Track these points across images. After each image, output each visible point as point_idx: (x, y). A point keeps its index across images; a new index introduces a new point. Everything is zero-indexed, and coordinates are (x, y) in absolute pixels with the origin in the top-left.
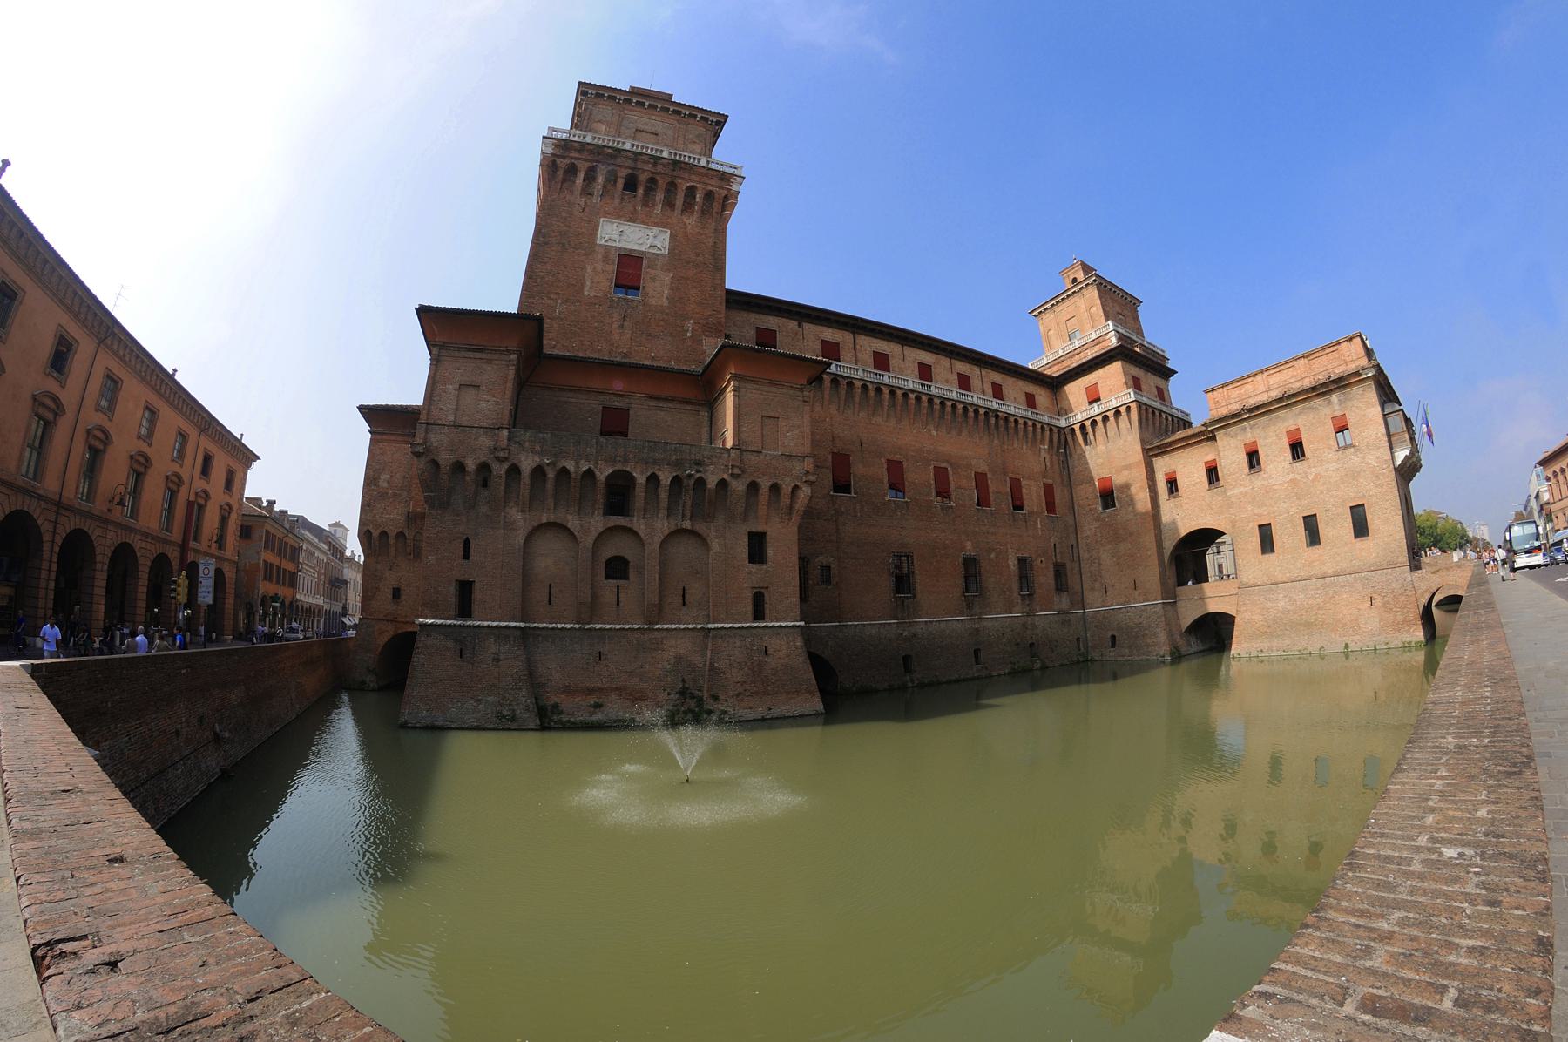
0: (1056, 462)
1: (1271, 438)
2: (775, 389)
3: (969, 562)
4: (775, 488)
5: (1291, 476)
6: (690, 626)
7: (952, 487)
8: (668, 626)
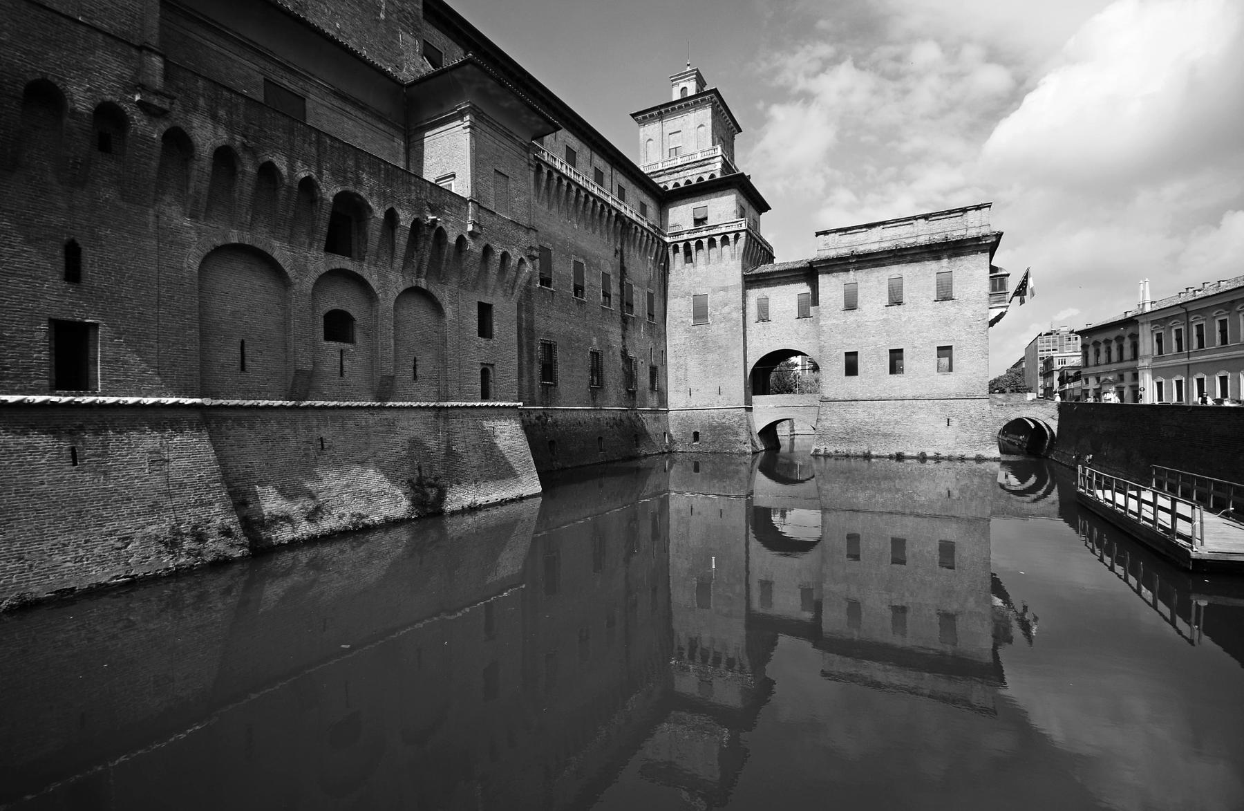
0: (657, 274)
1: (872, 283)
2: (505, 141)
3: (596, 356)
4: (505, 256)
5: (885, 316)
6: (423, 404)
7: (586, 282)
8: (400, 404)
